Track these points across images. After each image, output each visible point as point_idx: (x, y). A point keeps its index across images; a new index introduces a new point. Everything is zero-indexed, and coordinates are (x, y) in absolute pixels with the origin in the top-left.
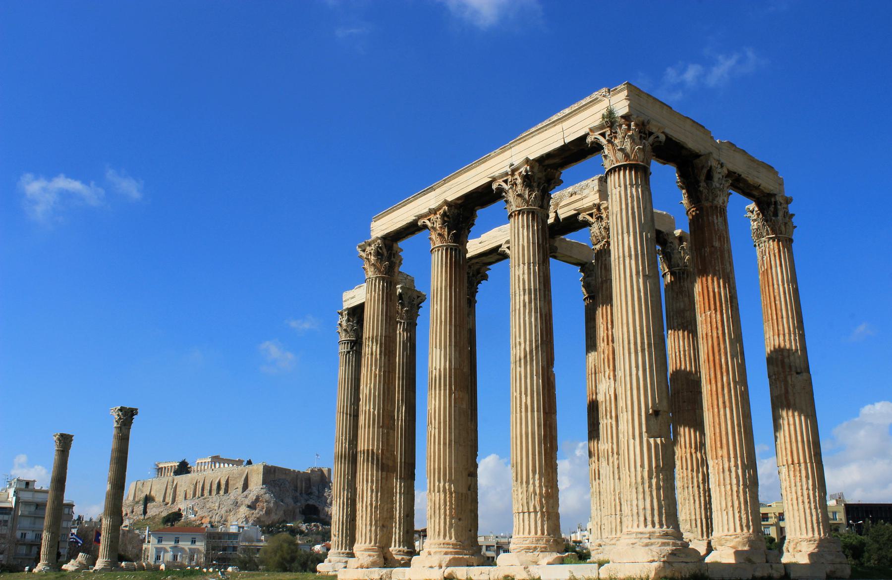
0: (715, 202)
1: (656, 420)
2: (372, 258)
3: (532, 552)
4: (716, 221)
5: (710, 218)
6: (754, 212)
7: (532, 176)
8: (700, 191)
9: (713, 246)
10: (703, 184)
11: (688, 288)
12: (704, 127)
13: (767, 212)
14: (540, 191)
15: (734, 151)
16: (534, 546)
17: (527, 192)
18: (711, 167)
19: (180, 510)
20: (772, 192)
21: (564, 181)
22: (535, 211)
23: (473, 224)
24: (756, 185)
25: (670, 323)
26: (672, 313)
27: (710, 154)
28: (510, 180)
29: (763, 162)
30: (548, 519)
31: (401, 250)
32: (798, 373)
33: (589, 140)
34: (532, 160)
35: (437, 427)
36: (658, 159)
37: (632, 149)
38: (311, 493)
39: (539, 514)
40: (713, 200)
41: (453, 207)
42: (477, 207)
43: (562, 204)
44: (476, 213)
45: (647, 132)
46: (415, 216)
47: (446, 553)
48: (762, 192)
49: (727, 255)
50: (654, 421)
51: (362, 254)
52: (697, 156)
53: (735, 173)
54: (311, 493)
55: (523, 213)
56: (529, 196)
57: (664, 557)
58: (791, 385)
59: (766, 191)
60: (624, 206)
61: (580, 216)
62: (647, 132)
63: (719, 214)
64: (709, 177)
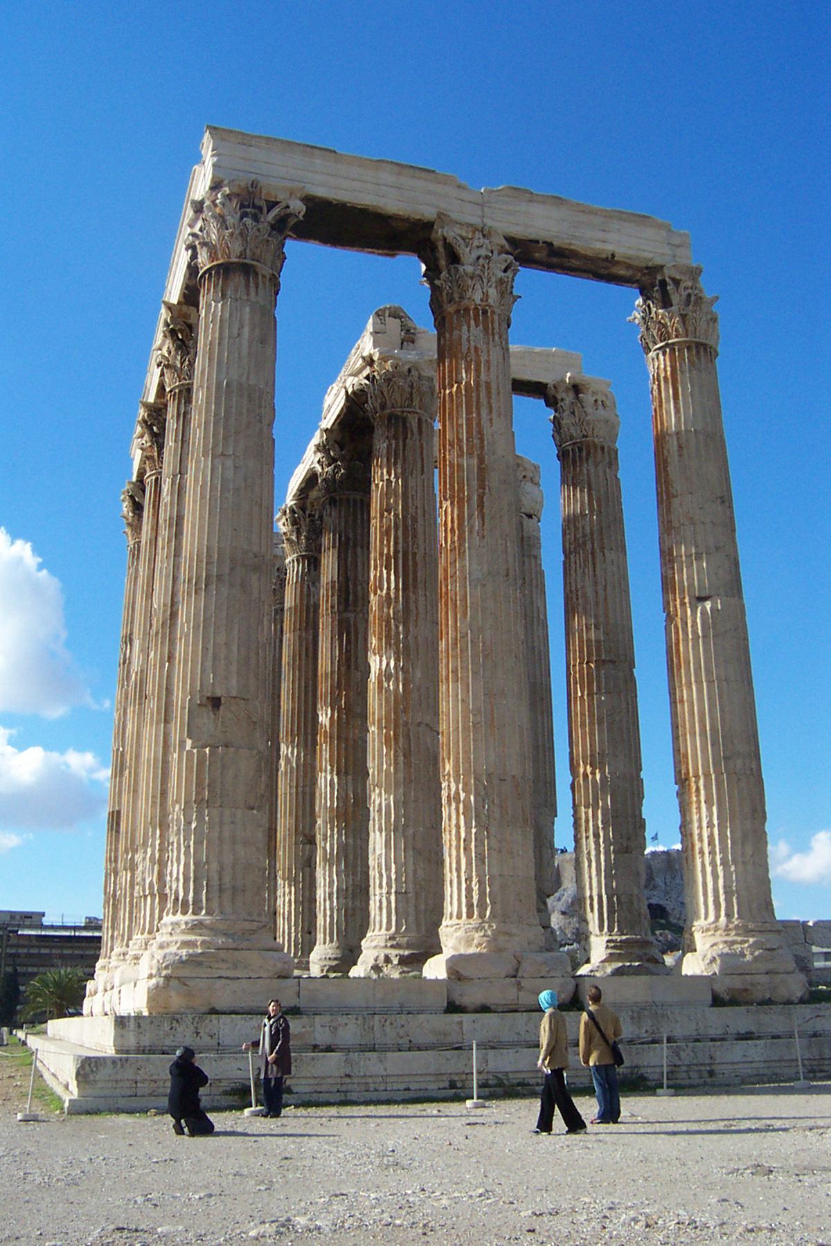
1: (215, 714)
4: (465, 337)
5: (456, 332)
10: (444, 274)
11: (588, 474)
15: (530, 201)
20: (650, 264)
34: (179, 303)
37: (221, 237)
38: (655, 887)
40: (462, 298)
45: (263, 204)
48: (629, 267)
50: (209, 718)
53: (538, 242)
54: (655, 887)
57: (166, 967)
59: (636, 263)
62: (263, 204)
63: (472, 322)
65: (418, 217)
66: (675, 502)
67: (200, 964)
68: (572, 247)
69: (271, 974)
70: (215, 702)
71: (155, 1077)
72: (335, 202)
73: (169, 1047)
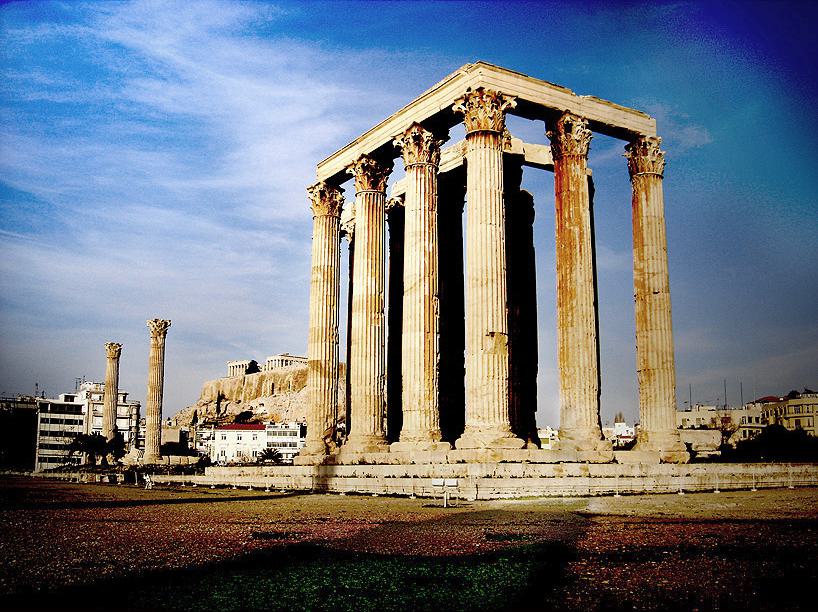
0: (573, 152)
2: (318, 200)
10: (563, 136)
19: (252, 408)
27: (567, 112)
31: (344, 190)
32: (655, 293)
33: (455, 108)
51: (311, 196)
64: (569, 128)
66: (646, 248)
70: (492, 334)
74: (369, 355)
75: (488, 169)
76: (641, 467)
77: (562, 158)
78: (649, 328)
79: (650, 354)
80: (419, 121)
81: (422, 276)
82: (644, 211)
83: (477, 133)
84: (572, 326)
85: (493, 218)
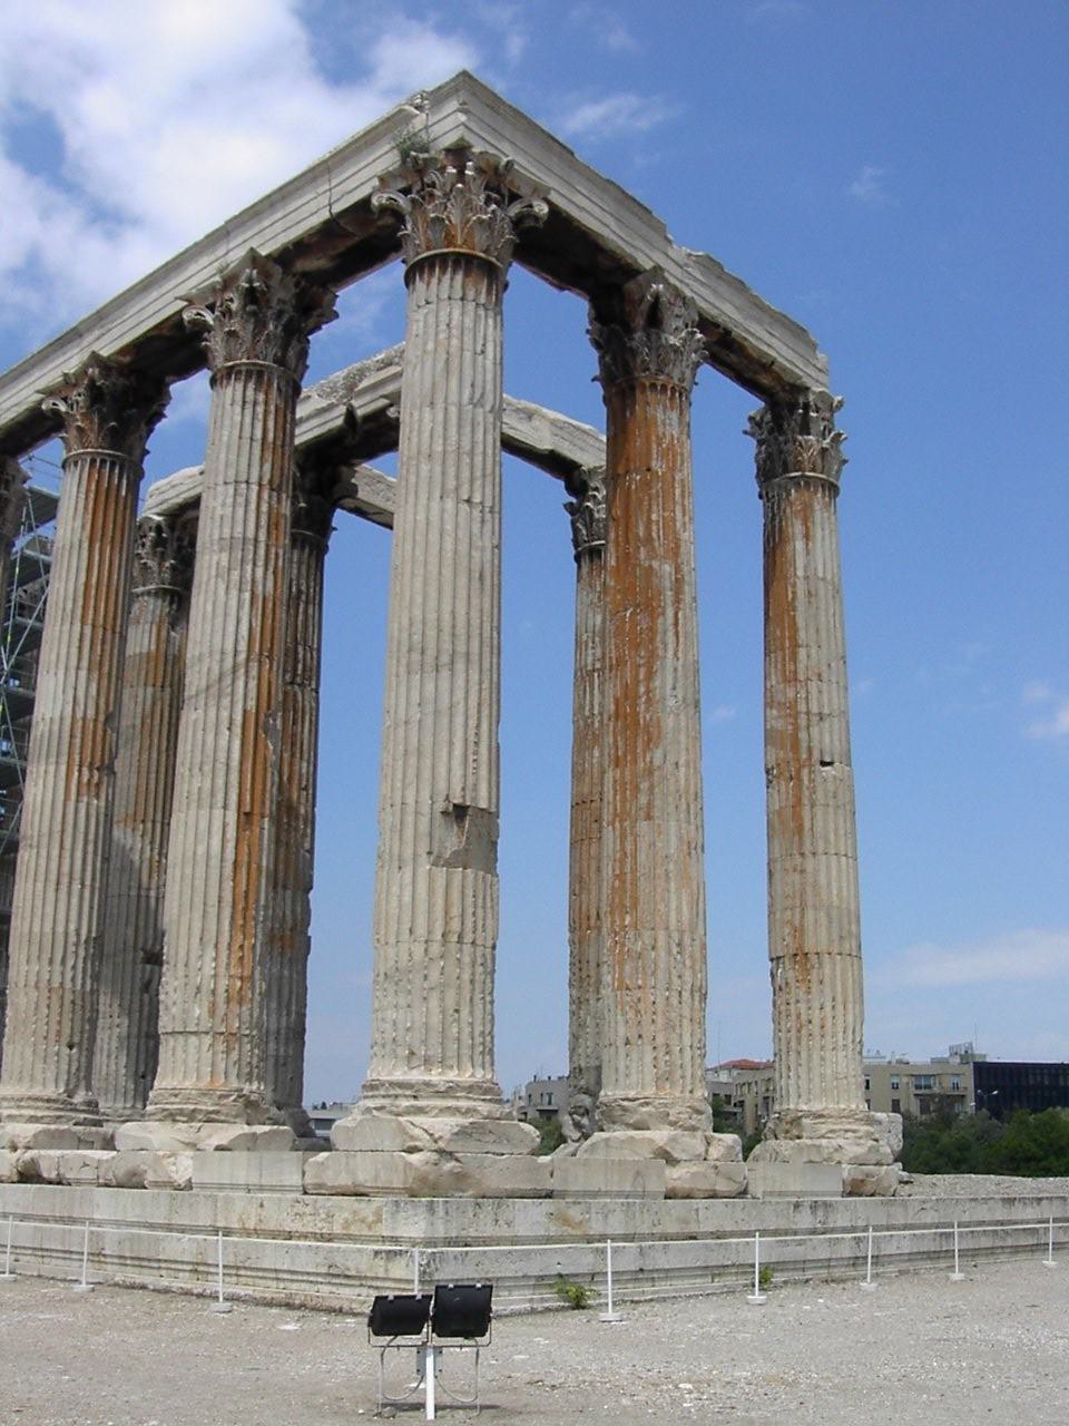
3: (186, 1122)
4: (660, 416)
6: (764, 424)
7: (264, 293)
8: (631, 349)
9: (649, 470)
10: (639, 335)
12: (649, 212)
13: (789, 425)
14: (280, 328)
15: (719, 277)
16: (192, 1107)
17: (251, 327)
18: (657, 297)
20: (799, 382)
21: (341, 315)
22: (263, 369)
23: (160, 416)
24: (764, 361)
25: (581, 654)
26: (584, 638)
28: (218, 304)
29: (784, 316)
30: (228, 1052)
32: (824, 764)
34: (269, 256)
35: (35, 844)
36: (544, 275)
39: (207, 1040)
40: (660, 371)
41: (114, 371)
42: (171, 378)
43: (361, 386)
44: (168, 392)
46: (38, 392)
47: (33, 1119)
48: (778, 378)
49: (678, 492)
52: (631, 271)
53: (717, 326)
55: (239, 372)
56: (254, 338)
58: (808, 788)
59: (787, 378)
60: (430, 346)
61: (392, 409)
62: (507, 194)
64: (655, 319)
65: (629, 261)
66: (802, 652)
67: (471, 1135)
68: (746, 343)
69: (525, 1152)
70: (459, 812)
71: (490, 1275)
72: (564, 214)
73: (473, 1238)
74: (65, 880)
75: (468, 355)
76: (814, 1206)
77: (633, 389)
78: (807, 848)
79: (810, 915)
80: (264, 252)
81: (242, 657)
82: (800, 563)
83: (443, 258)
84: (649, 817)
85: (478, 483)
